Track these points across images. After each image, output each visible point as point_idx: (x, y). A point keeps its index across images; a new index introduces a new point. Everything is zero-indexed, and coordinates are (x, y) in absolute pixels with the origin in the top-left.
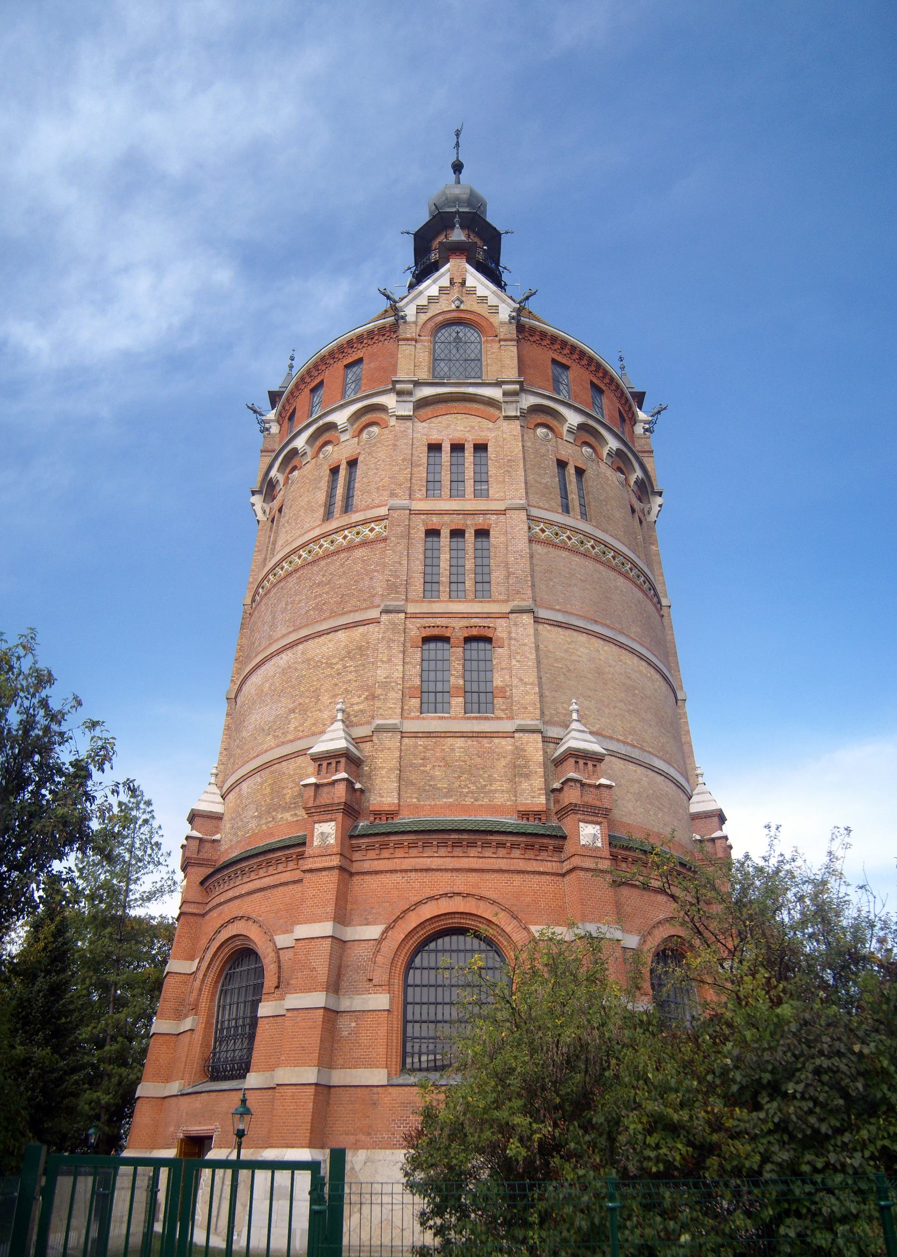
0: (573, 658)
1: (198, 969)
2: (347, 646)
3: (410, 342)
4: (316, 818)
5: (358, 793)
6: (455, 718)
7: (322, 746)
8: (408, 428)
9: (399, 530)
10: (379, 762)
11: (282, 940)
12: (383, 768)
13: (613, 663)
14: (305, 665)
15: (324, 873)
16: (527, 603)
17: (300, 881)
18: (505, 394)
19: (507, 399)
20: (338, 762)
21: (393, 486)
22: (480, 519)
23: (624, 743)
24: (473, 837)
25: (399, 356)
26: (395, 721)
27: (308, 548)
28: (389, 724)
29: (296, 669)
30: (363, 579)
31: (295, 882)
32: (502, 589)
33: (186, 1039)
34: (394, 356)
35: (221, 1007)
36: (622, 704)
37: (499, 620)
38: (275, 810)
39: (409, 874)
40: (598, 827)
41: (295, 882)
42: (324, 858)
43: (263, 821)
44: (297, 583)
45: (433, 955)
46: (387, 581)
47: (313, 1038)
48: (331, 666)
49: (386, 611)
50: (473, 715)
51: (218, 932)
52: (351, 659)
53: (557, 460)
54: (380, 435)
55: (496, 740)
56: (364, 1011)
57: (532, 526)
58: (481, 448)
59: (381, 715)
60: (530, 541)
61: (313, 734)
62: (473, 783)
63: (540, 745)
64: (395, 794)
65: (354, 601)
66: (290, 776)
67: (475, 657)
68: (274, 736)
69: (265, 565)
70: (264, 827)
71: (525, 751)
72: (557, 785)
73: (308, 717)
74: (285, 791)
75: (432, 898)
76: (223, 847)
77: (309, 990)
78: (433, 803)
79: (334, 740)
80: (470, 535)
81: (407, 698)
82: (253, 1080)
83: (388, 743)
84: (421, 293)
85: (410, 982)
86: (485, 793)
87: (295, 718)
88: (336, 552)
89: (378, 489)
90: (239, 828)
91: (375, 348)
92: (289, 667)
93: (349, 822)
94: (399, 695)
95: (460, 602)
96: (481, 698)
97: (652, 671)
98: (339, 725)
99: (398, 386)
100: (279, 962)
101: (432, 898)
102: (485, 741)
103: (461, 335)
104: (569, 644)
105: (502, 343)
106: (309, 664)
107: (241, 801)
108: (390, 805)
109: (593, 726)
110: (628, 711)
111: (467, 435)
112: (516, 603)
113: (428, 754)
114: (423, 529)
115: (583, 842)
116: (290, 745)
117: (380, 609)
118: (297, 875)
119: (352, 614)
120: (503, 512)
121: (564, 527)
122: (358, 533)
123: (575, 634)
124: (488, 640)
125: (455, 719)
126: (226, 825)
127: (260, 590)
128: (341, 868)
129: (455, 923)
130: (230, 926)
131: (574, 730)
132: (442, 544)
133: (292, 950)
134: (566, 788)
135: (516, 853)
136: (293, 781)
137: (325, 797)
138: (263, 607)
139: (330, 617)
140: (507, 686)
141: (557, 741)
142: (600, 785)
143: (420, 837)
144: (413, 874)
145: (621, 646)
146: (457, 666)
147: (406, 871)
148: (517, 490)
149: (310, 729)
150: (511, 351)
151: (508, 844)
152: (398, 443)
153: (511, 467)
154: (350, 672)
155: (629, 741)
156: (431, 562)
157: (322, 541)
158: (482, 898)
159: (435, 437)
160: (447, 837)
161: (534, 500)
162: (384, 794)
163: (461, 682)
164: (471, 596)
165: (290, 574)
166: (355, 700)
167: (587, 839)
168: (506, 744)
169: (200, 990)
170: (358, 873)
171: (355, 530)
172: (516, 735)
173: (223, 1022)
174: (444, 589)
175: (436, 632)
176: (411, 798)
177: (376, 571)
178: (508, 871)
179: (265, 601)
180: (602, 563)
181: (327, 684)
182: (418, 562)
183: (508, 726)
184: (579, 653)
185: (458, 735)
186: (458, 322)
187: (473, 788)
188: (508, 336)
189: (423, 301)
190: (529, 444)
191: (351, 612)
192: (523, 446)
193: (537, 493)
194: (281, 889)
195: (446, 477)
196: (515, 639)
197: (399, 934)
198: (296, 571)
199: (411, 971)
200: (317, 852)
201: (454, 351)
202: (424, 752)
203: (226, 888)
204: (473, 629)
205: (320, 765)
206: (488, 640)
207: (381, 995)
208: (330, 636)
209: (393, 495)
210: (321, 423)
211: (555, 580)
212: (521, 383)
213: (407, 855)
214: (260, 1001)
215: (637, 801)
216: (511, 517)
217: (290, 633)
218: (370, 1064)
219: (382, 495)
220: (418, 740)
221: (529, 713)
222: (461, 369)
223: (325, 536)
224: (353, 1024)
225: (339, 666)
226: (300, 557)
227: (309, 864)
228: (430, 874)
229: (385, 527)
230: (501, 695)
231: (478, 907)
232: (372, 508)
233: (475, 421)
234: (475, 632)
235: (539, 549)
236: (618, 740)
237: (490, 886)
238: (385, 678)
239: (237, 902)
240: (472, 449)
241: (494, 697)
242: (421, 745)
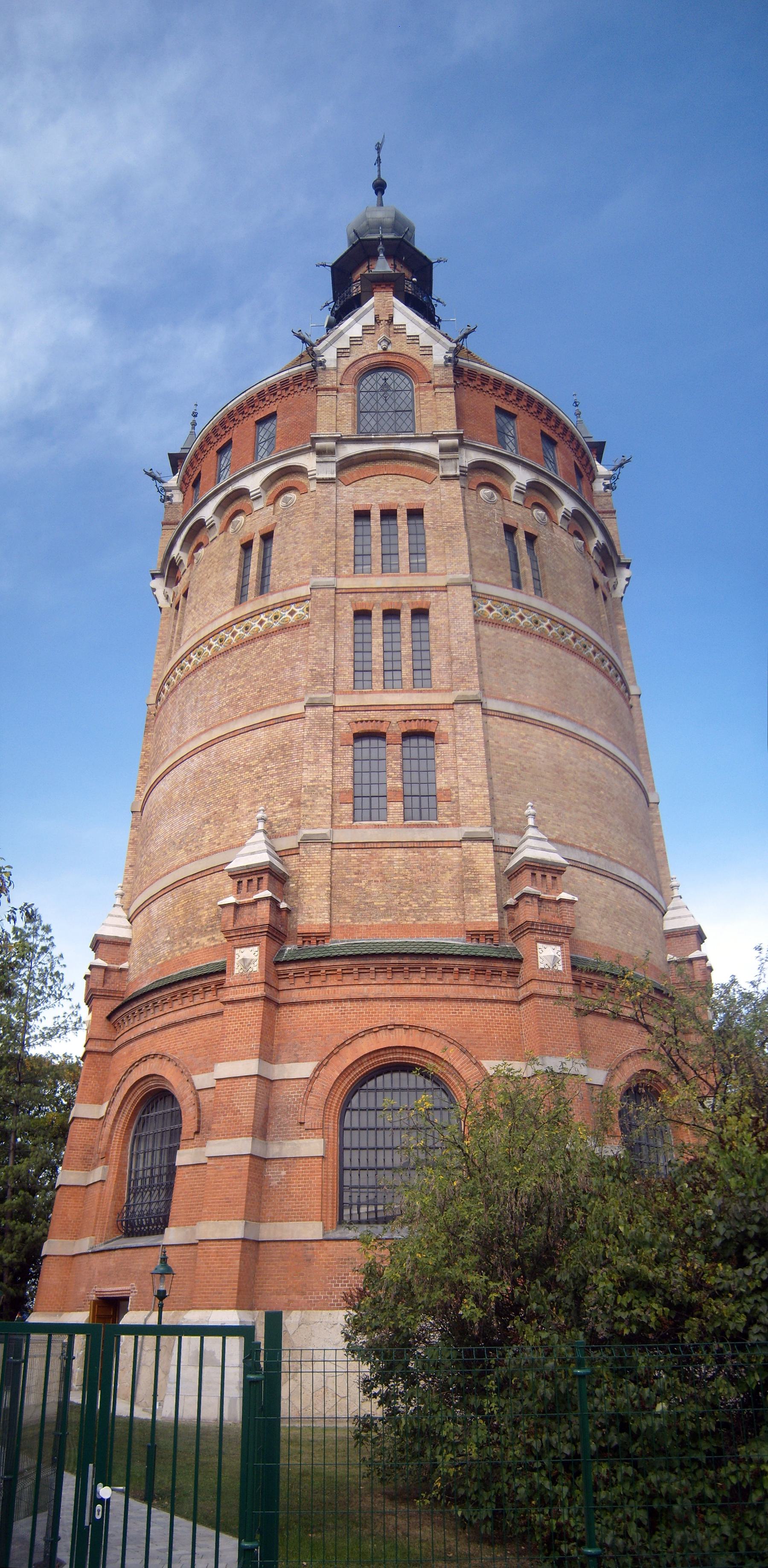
0: (529, 754)
1: (107, 1113)
2: (267, 746)
3: (330, 392)
4: (236, 943)
5: (284, 913)
6: (393, 826)
7: (241, 860)
8: (330, 493)
9: (324, 611)
10: (307, 878)
11: (202, 1080)
12: (311, 884)
13: (575, 760)
14: (220, 768)
15: (247, 1004)
16: (474, 693)
17: (220, 1013)
18: (442, 450)
19: (445, 456)
20: (260, 879)
21: (315, 562)
22: (418, 597)
23: (588, 851)
24: (416, 961)
25: (319, 409)
26: (325, 830)
27: (219, 636)
28: (318, 835)
29: (210, 773)
30: (283, 669)
31: (214, 1015)
32: (445, 677)
33: (96, 1191)
34: (312, 409)
35: (135, 1156)
36: (585, 807)
37: (442, 712)
38: (189, 934)
39: (344, 1004)
40: (558, 948)
41: (214, 1015)
42: (246, 988)
43: (176, 948)
44: (208, 677)
45: (372, 1095)
47: (239, 1189)
48: (249, 768)
49: (311, 705)
50: (414, 822)
51: (128, 1072)
52: (272, 760)
53: (505, 525)
54: (299, 502)
55: (441, 851)
56: (295, 1158)
57: (478, 604)
58: (415, 514)
59: (309, 824)
60: (476, 621)
61: (231, 847)
62: (414, 900)
63: (491, 855)
64: (326, 914)
65: (273, 695)
66: (206, 896)
67: (414, 754)
68: (186, 850)
69: (170, 658)
70: (178, 954)
71: (474, 862)
72: (511, 901)
73: (225, 827)
74: (200, 913)
75: (370, 1031)
76: (131, 978)
77: (234, 1136)
78: (370, 923)
79: (255, 853)
80: (406, 616)
81: (338, 804)
82: (172, 1235)
83: (317, 857)
84: (342, 333)
85: (347, 1124)
86: (429, 911)
87: (210, 829)
88: (252, 640)
89: (297, 565)
90: (149, 955)
91: (290, 401)
92: (202, 771)
93: (274, 946)
94: (328, 801)
95: (396, 692)
96: (422, 803)
97: (620, 769)
98: (261, 836)
99: (318, 445)
100: (199, 1104)
101: (370, 1031)
102: (428, 851)
103: (389, 382)
104: (523, 738)
106: (224, 767)
107: (151, 924)
108: (320, 926)
109: (552, 833)
110: (593, 815)
111: (399, 499)
112: (460, 692)
113: (362, 868)
114: (351, 611)
115: (541, 966)
116: (205, 860)
117: (304, 703)
118: (217, 1007)
119: (272, 710)
120: (445, 589)
121: (515, 605)
122: (276, 617)
123: (530, 727)
124: (430, 735)
125: (392, 827)
126: (135, 952)
127: (166, 687)
128: (266, 999)
129: (397, 1059)
130: (142, 1065)
131: (530, 837)
132: (374, 626)
133: (211, 1091)
134: (521, 904)
135: (466, 979)
136: (209, 901)
137: (247, 918)
138: (169, 705)
139: (247, 714)
140: (452, 788)
141: (511, 851)
142: (561, 901)
143: (355, 962)
144: (348, 1005)
145: (584, 741)
146: (394, 766)
147: (340, 1001)
148: (459, 563)
149: (227, 841)
150: (448, 400)
151: (456, 969)
152: (320, 511)
153: (452, 536)
154: (272, 776)
155: (593, 848)
156: (361, 647)
157: (235, 628)
158: (426, 1030)
159: (362, 503)
160: (386, 961)
161: (480, 573)
162: (313, 914)
163: (399, 784)
164: (408, 685)
165: (199, 668)
166: (279, 807)
167: (545, 962)
168: (453, 855)
169: (111, 1137)
170: (285, 1004)
171: (272, 614)
172: (464, 844)
173: (137, 1172)
174: (377, 678)
175: (369, 727)
176: (344, 918)
177: (298, 660)
178: (456, 1000)
179: (171, 699)
180: (561, 646)
181: (246, 789)
182: (346, 649)
183: (455, 834)
184: (535, 749)
185: (397, 845)
186: (386, 367)
187: (415, 905)
188: (445, 382)
189: (344, 343)
190: (471, 508)
191: (271, 707)
192: (465, 511)
193: (483, 566)
194: (198, 1022)
195: (376, 550)
196: (461, 734)
197: (333, 1072)
198: (206, 663)
199: (348, 1113)
200: (238, 981)
201: (382, 401)
202: (359, 866)
203: (137, 1023)
204: (413, 723)
205: (239, 882)
206: (430, 735)
207: (315, 1140)
208: (247, 734)
209: (315, 572)
210: (230, 489)
211: (506, 666)
212: (460, 437)
213: (340, 983)
214: (178, 1147)
215: (603, 918)
216: (453, 595)
217: (201, 733)
218: (304, 1217)
219: (302, 573)
220: (351, 852)
221: (478, 818)
222: (391, 422)
223: (238, 621)
224: (284, 1173)
225: (259, 769)
226: (210, 647)
227: (230, 995)
228: (367, 1003)
229: (308, 609)
230: (446, 798)
231: (422, 1041)
232: (291, 588)
233: (407, 483)
234: (414, 727)
235: (487, 631)
236: (581, 849)
237: (437, 1016)
238: (312, 781)
239: (149, 1038)
240: (406, 516)
241: (437, 801)
242: (354, 858)
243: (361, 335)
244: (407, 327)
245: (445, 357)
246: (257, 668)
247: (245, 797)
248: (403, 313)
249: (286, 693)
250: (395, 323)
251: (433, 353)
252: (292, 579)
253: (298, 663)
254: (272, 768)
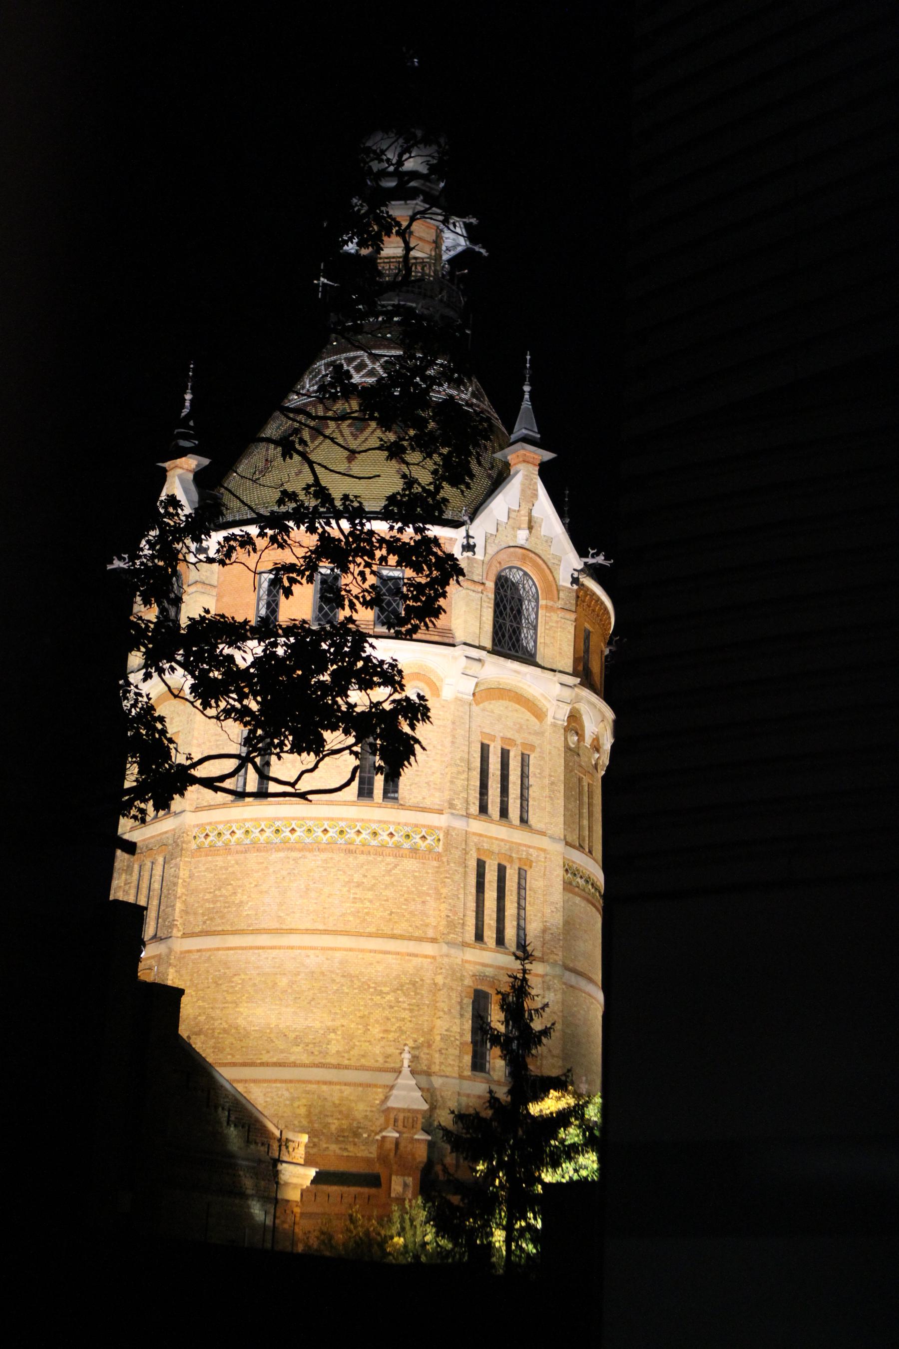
2: (398, 976)
29: (333, 981)
46: (448, 916)
48: (381, 993)
74: (330, 1120)
94: (457, 1052)
150: (569, 632)
177: (428, 895)
246: (386, 887)
247: (377, 1021)
249: (417, 927)
252: (424, 798)
253: (428, 898)
254: (404, 1002)
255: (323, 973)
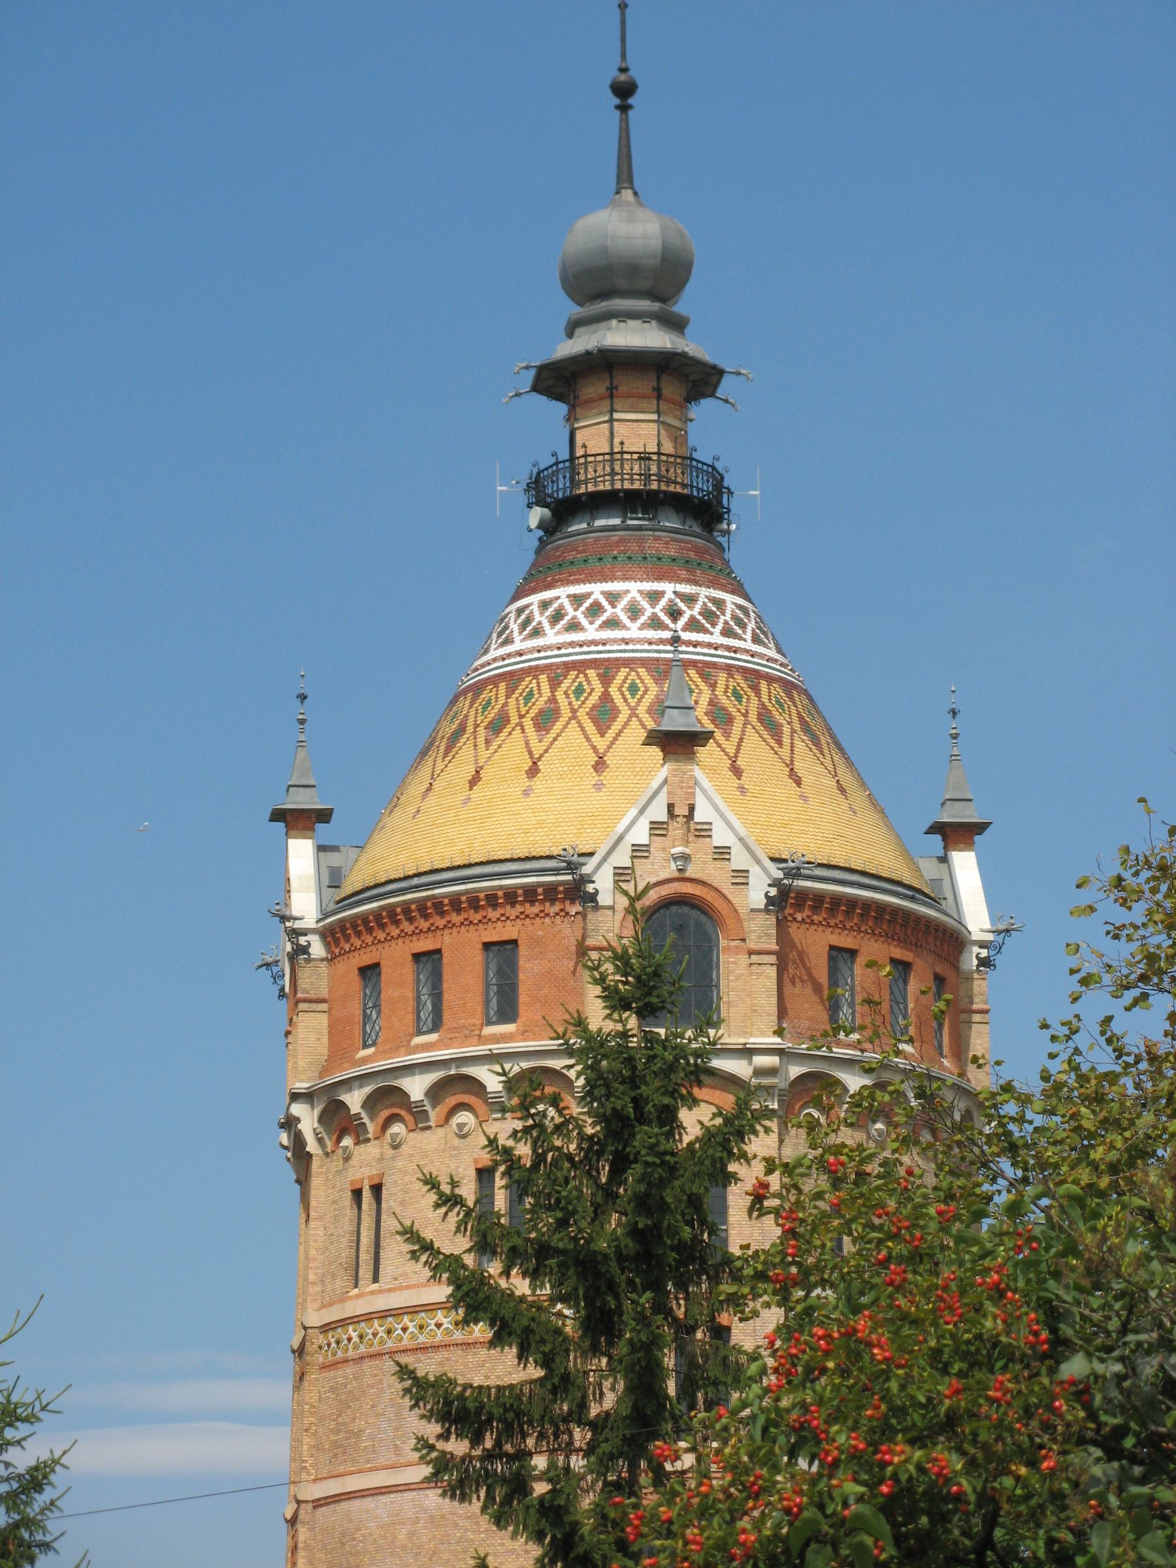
105: (754, 958)
150: (769, 977)
186: (682, 901)
188: (765, 947)
189: (622, 858)
243: (647, 842)
244: (713, 827)
245: (766, 895)
248: (709, 799)
250: (696, 819)
251: (751, 880)
255: (443, 1517)
